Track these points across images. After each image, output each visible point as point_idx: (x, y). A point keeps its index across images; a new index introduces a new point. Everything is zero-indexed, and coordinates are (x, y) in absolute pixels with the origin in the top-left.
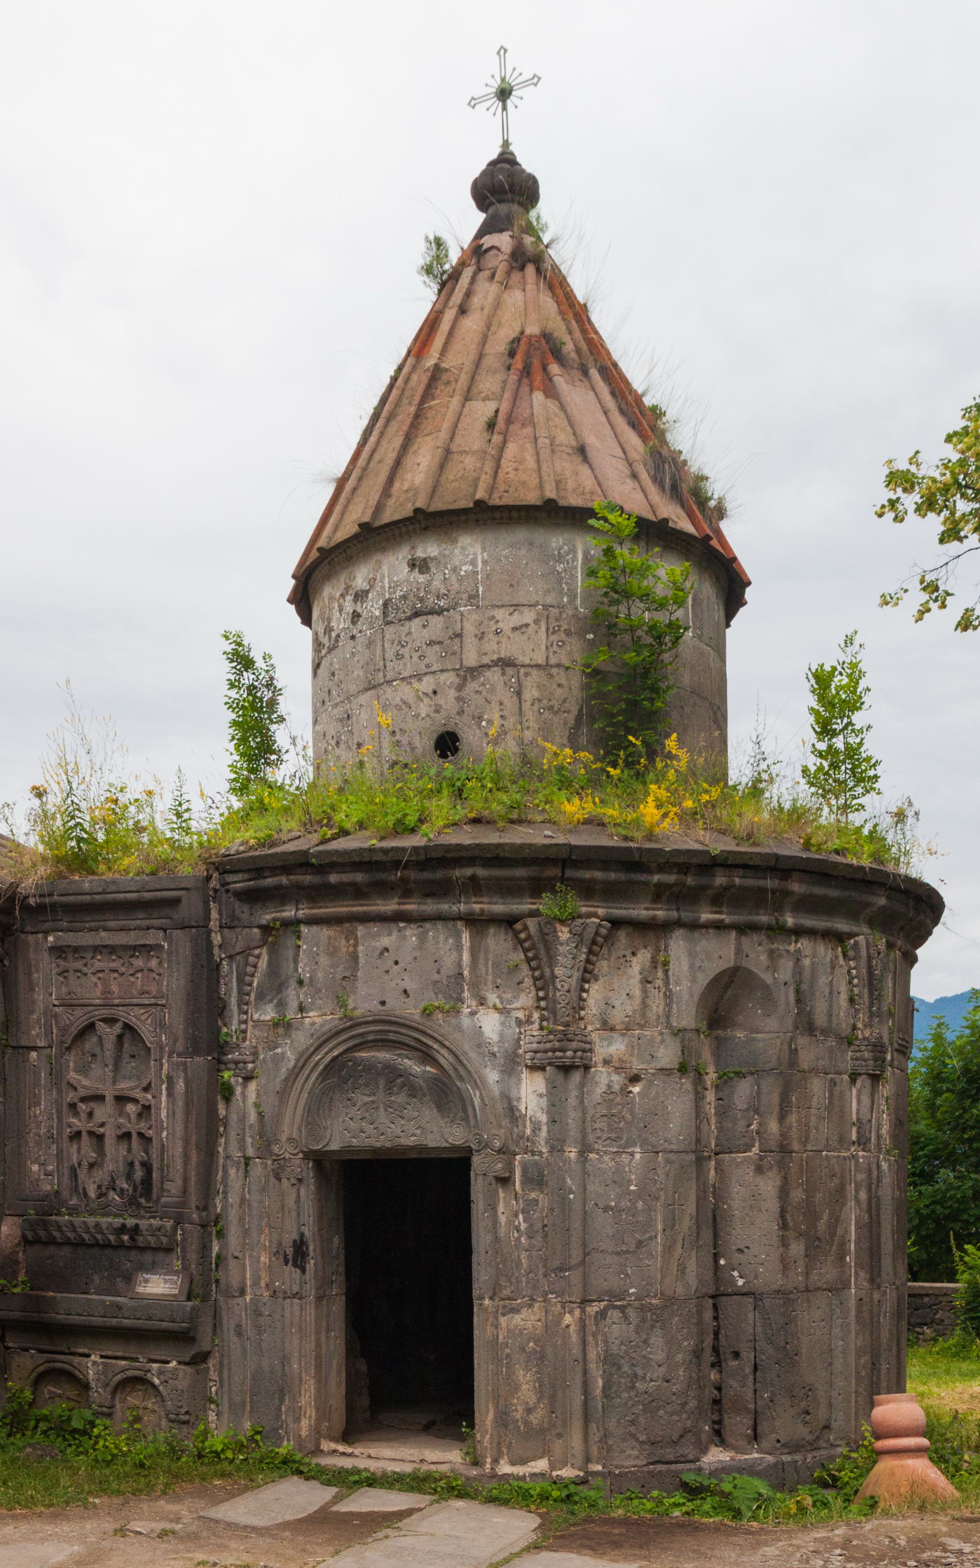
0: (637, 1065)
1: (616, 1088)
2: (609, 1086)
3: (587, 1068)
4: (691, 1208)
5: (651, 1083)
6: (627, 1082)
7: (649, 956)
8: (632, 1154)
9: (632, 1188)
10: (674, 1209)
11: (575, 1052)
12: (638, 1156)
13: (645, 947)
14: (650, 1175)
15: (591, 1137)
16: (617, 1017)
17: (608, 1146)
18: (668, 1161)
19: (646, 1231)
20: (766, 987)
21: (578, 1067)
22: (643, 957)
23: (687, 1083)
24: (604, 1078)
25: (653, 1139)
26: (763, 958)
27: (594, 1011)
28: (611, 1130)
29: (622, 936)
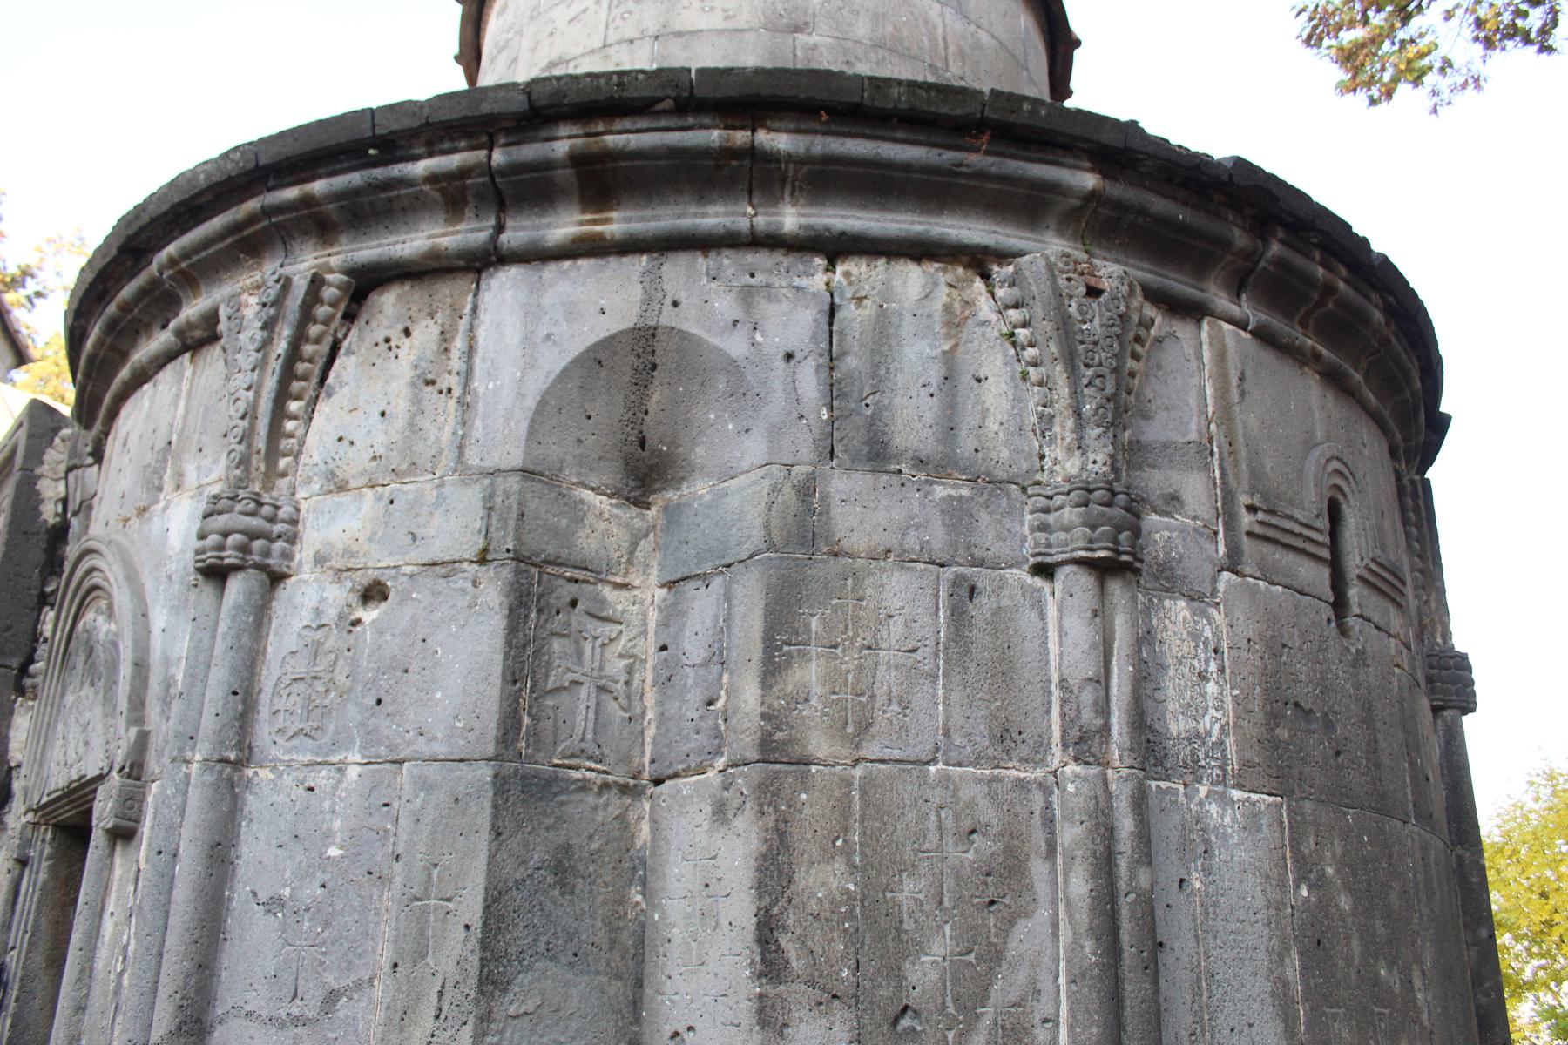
0: (377, 561)
1: (331, 614)
2: (318, 612)
3: (276, 578)
4: (471, 907)
5: (405, 597)
6: (354, 599)
7: (436, 330)
8: (341, 768)
9: (334, 852)
10: (424, 911)
11: (226, 535)
12: (353, 772)
13: (431, 315)
14: (374, 821)
15: (263, 731)
16: (355, 463)
17: (295, 749)
18: (425, 785)
19: (350, 966)
20: (733, 367)
21: (236, 568)
22: (426, 333)
23: (492, 593)
24: (311, 595)
25: (387, 727)
26: (725, 305)
27: (316, 459)
28: (309, 710)
29: (388, 301)
